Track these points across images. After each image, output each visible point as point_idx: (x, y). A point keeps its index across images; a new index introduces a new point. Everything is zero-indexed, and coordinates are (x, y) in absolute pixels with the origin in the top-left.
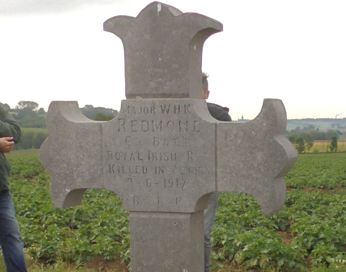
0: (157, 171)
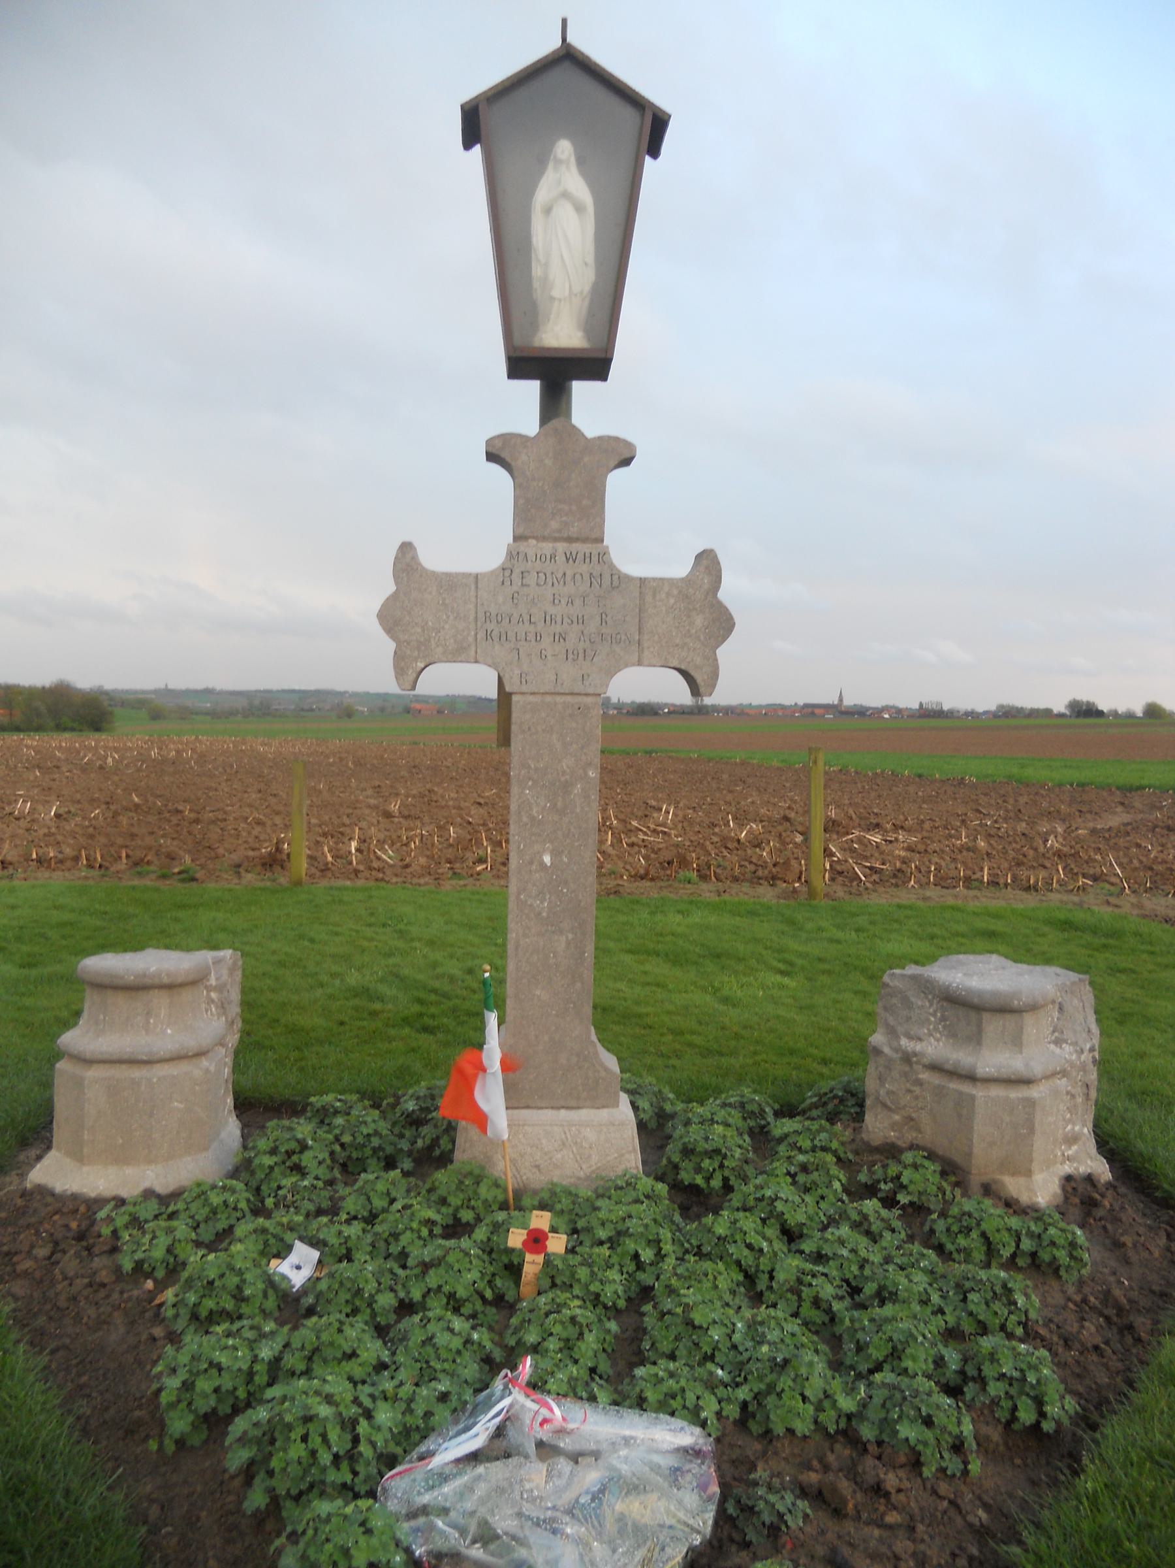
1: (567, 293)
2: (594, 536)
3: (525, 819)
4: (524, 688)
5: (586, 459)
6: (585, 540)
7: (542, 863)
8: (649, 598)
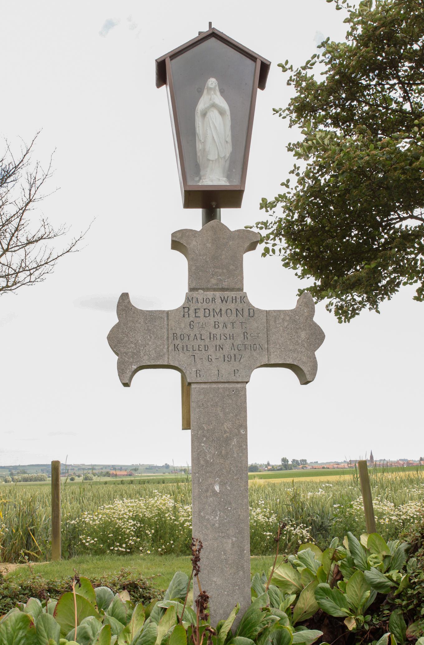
0: (218, 348)
2: (237, 287)
3: (202, 462)
4: (199, 380)
5: (231, 243)
6: (232, 290)
7: (214, 491)
8: (272, 323)
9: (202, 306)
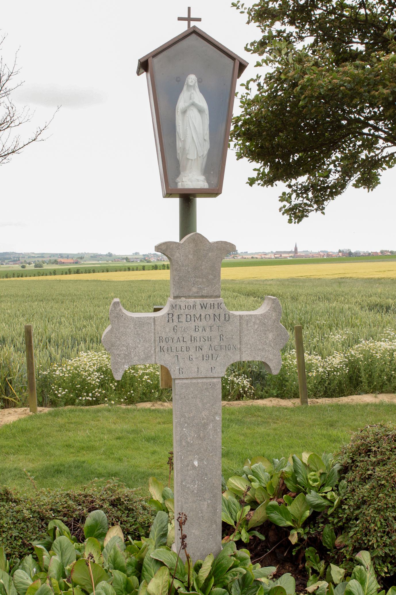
0: (197, 349)
1: (196, 157)
2: (215, 294)
3: (184, 444)
4: (181, 376)
6: (211, 297)
7: (193, 466)
8: (244, 326)
9: (184, 312)
